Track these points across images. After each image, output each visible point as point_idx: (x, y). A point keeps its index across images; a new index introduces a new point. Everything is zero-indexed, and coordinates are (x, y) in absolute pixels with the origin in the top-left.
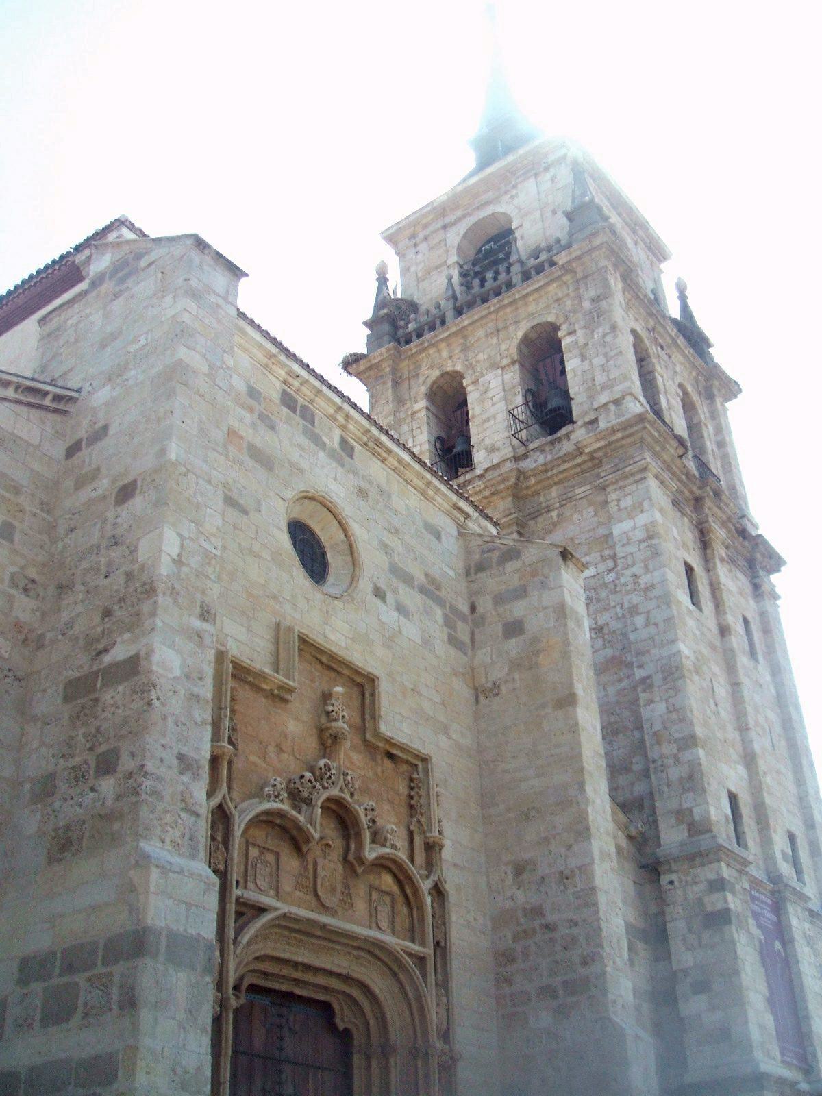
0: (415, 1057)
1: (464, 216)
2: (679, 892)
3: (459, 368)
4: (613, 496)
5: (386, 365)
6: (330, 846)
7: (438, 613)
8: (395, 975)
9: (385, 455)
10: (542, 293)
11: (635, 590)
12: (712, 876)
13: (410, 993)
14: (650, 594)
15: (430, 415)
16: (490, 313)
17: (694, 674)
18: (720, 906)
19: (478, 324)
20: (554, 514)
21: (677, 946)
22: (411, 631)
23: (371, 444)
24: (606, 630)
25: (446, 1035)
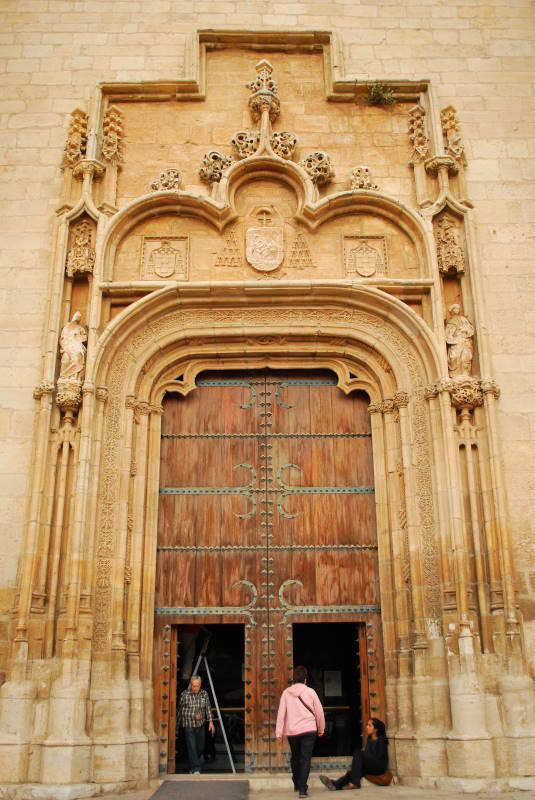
0: (427, 400)
6: (267, 213)
8: (386, 319)
13: (409, 332)
25: (474, 366)
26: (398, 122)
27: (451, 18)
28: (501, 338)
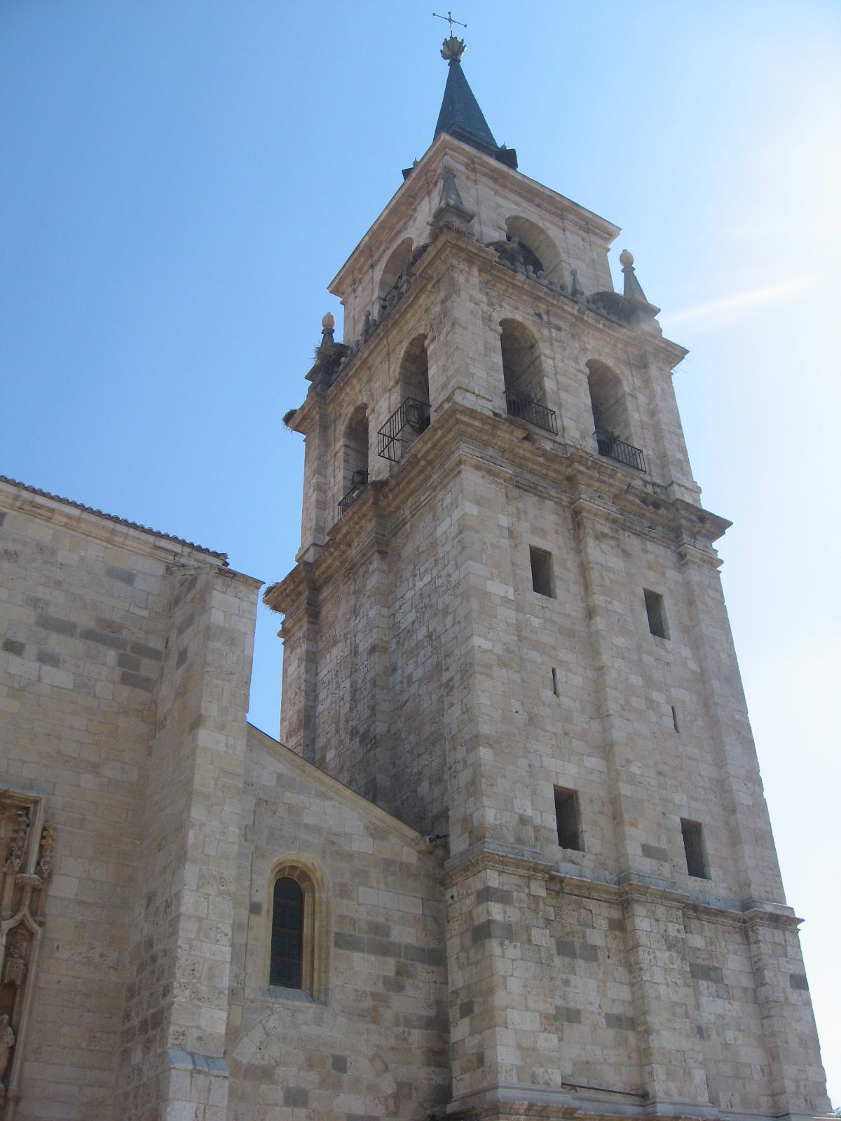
1: (384, 251)
2: (457, 906)
3: (365, 400)
4: (440, 496)
5: (314, 412)
7: (111, 655)
9: (49, 514)
10: (416, 307)
11: (448, 589)
12: (480, 886)
14: (458, 592)
15: (350, 452)
16: (381, 339)
17: (497, 671)
18: (483, 919)
19: (376, 353)
20: (408, 525)
21: (452, 964)
22: (61, 678)
23: (27, 507)
24: (434, 637)
26: (6, 826)
27: (80, 730)
28: (37, 1046)
